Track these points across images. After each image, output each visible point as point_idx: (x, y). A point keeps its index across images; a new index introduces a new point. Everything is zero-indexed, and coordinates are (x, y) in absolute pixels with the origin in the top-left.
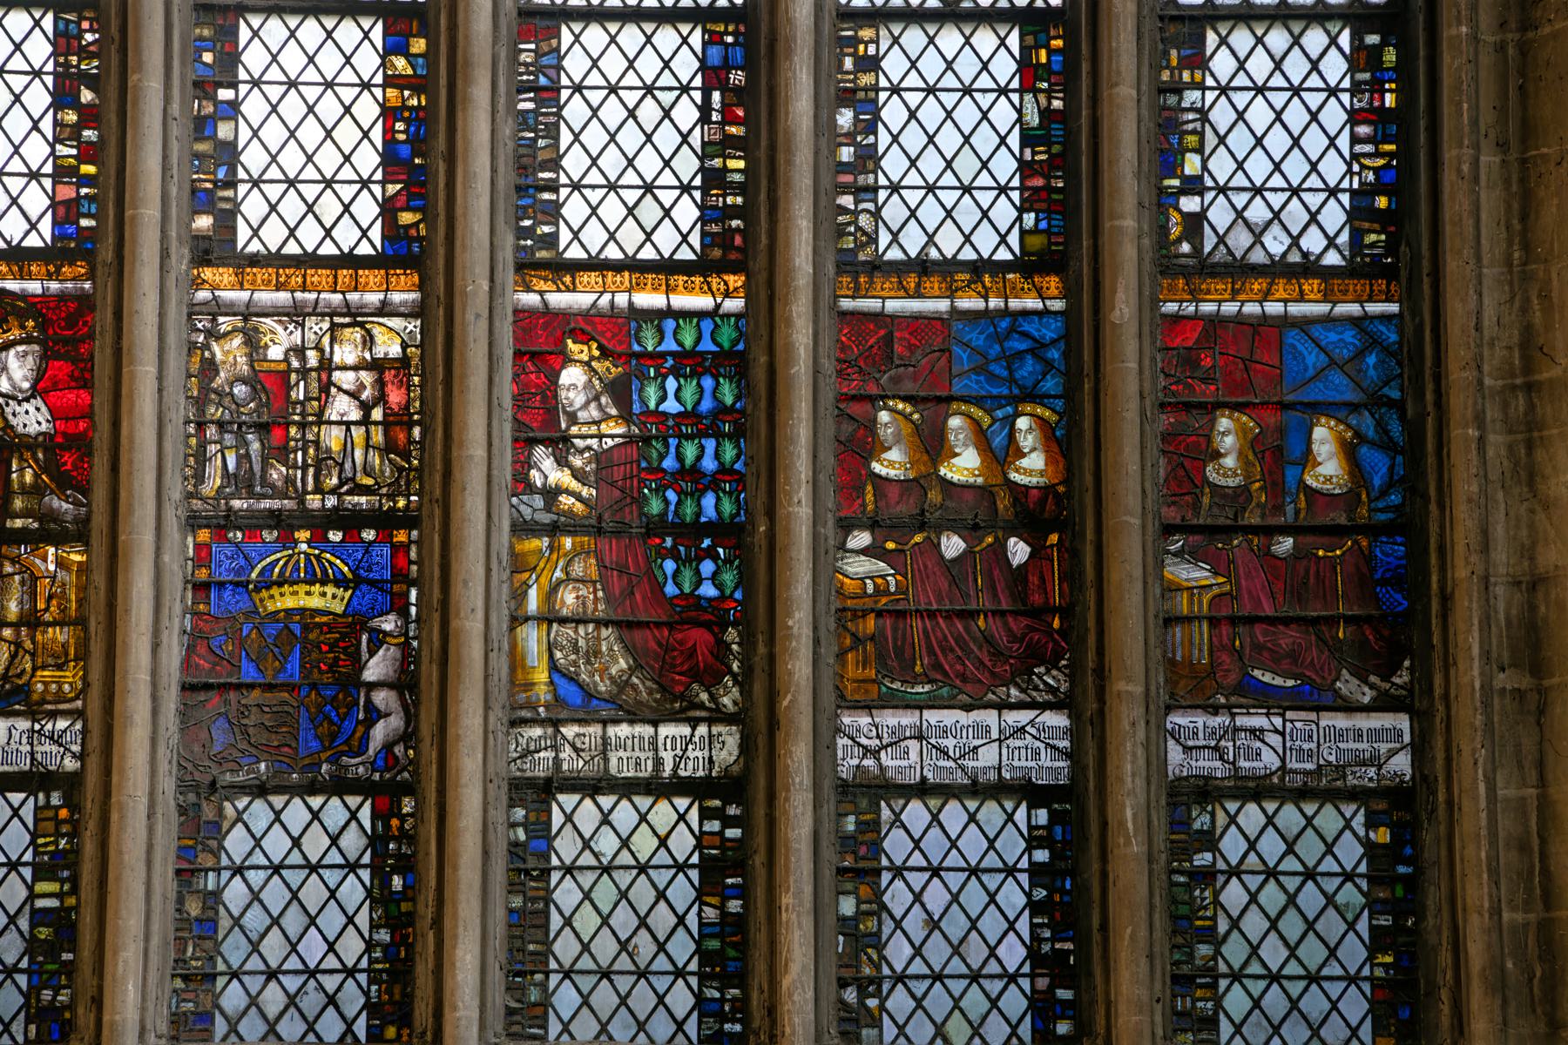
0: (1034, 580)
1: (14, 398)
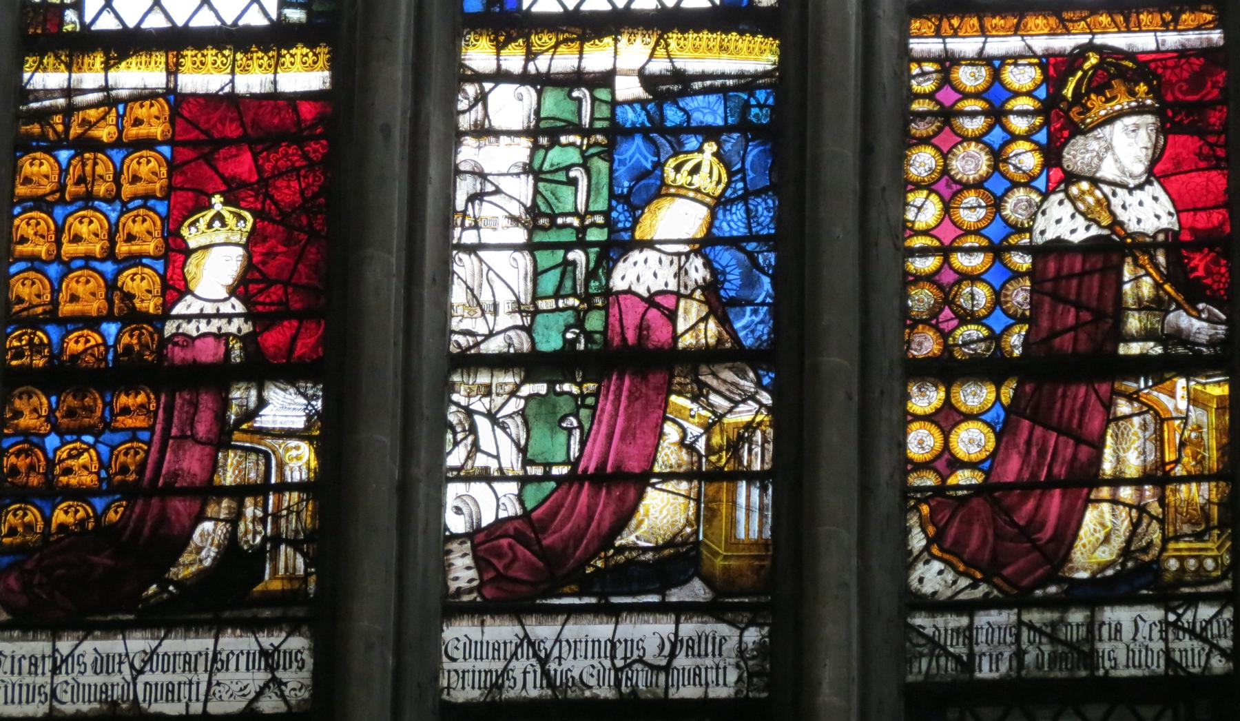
1: (1123, 186)
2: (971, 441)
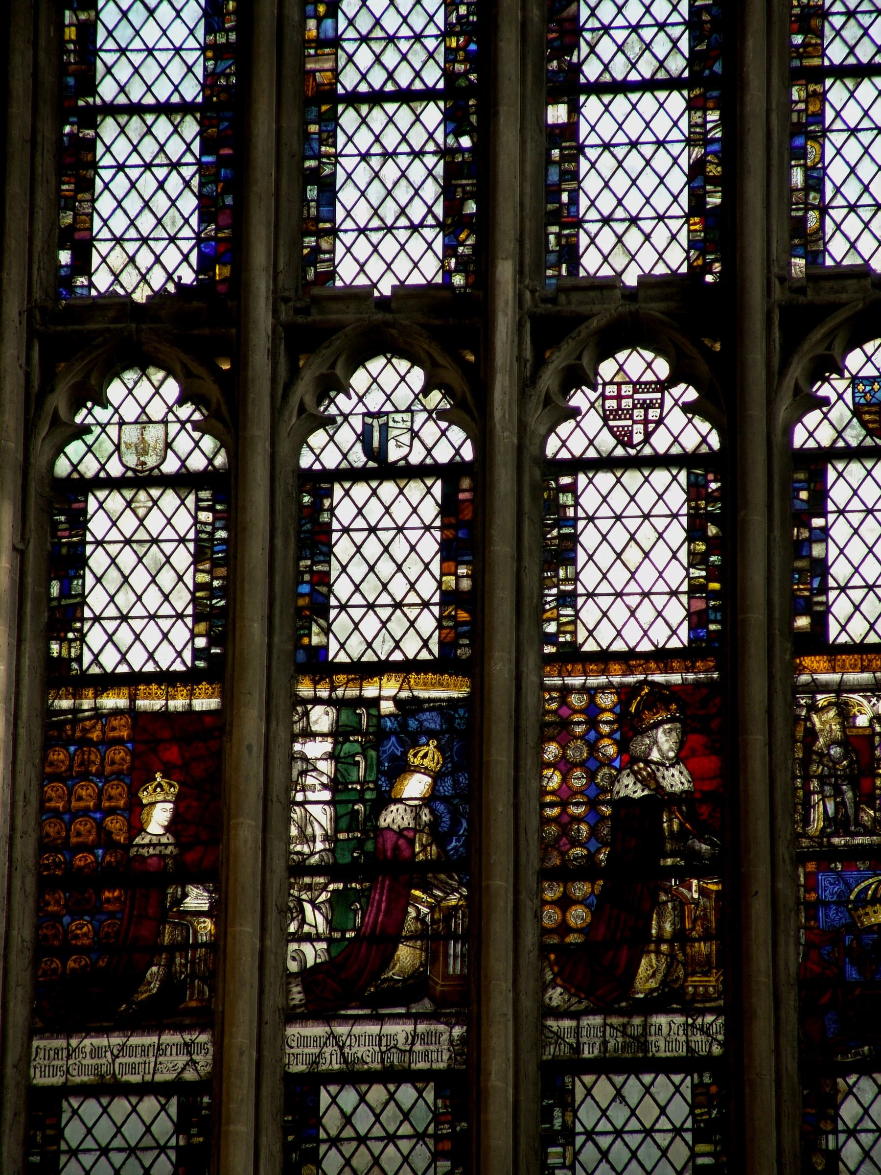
1: (663, 765)
2: (578, 916)
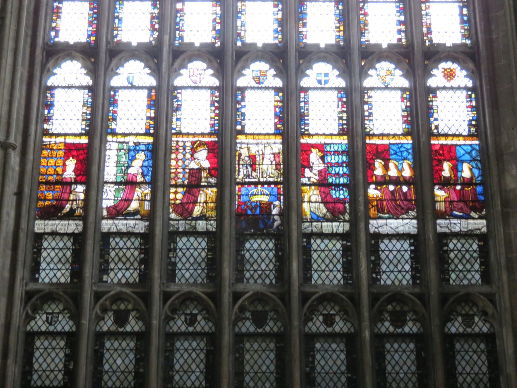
0: (408, 194)
